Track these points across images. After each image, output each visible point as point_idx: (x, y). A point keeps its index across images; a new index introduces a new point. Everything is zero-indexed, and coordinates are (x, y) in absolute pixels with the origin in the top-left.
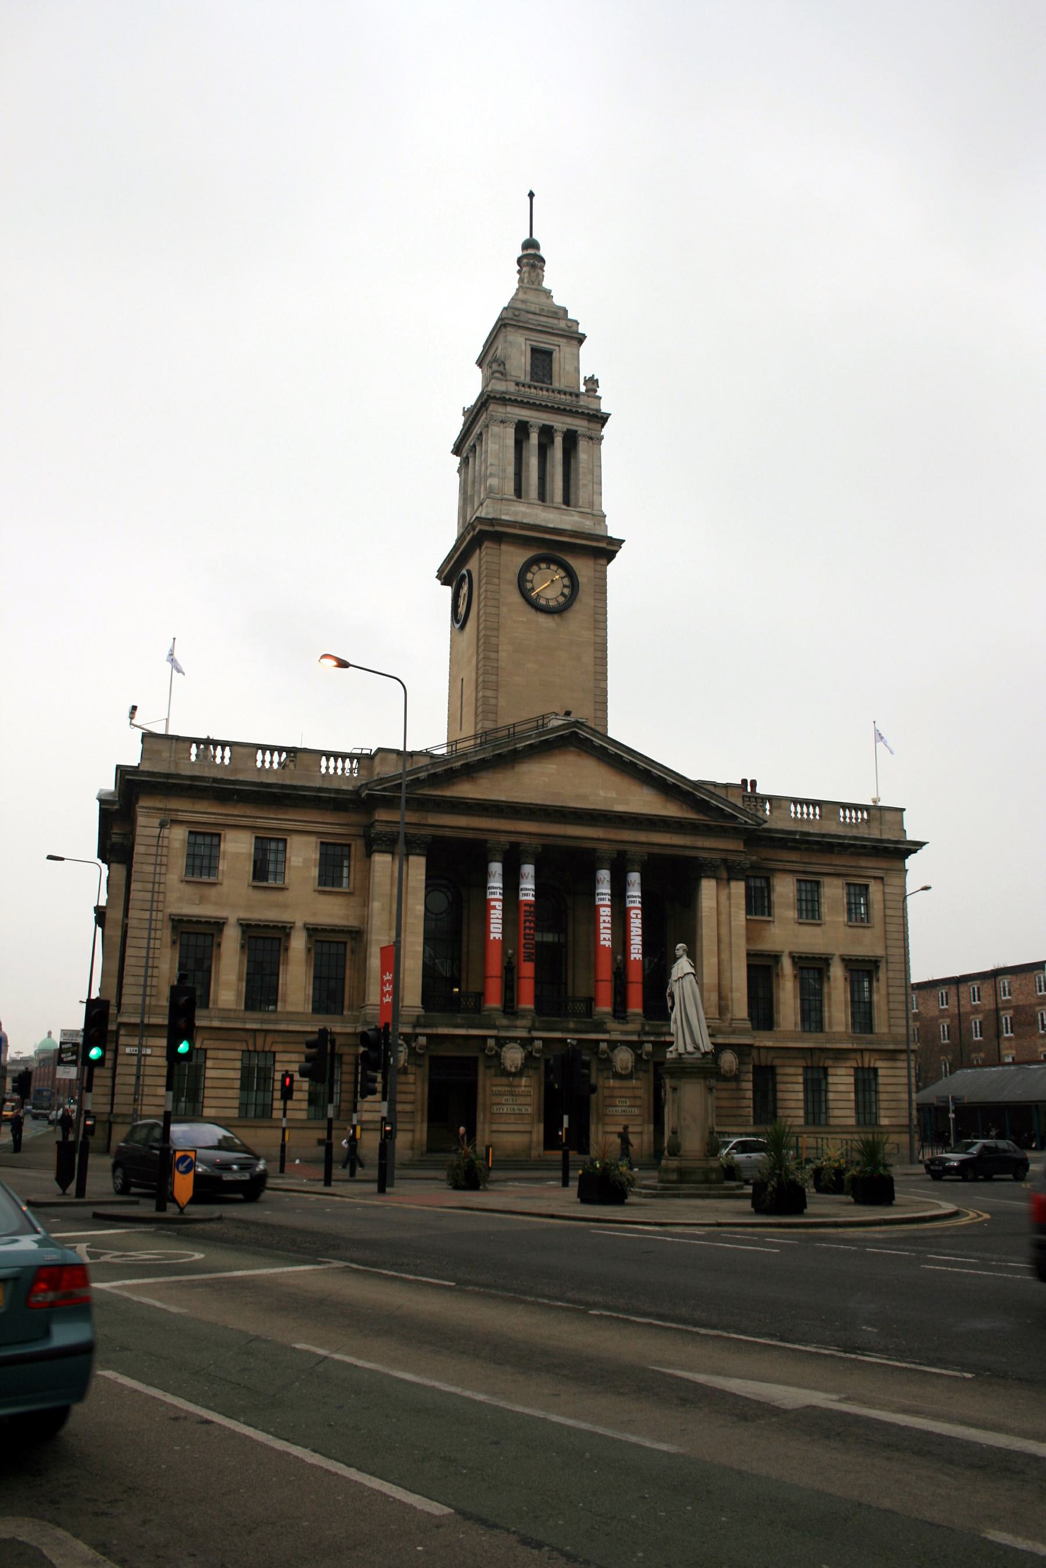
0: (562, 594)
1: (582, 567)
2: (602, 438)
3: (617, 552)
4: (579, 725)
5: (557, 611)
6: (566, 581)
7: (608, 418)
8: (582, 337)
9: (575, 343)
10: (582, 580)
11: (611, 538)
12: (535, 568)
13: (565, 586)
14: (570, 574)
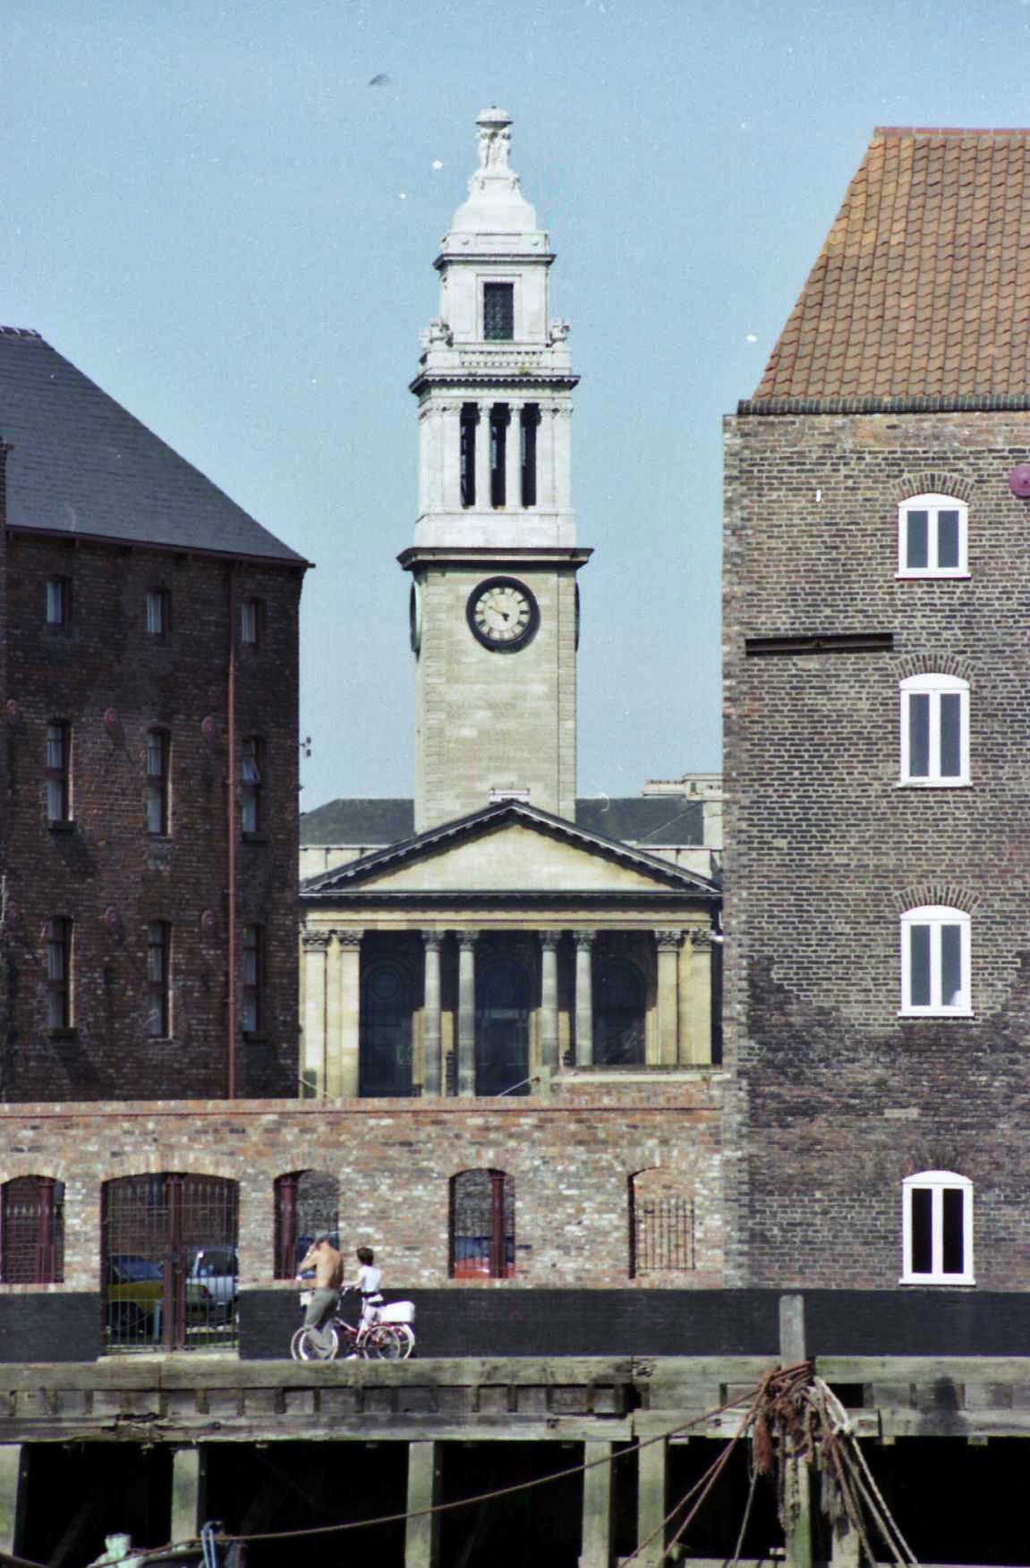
0: (519, 623)
5: (515, 645)
6: (525, 606)
10: (541, 601)
12: (485, 597)
13: (522, 612)
14: (528, 595)
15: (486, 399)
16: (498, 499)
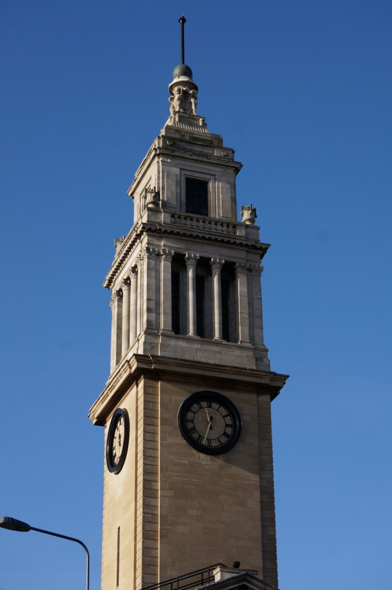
0: (225, 434)
1: (244, 402)
2: (260, 270)
3: (280, 388)
4: (250, 579)
7: (267, 249)
8: (238, 166)
9: (231, 171)
11: (275, 374)
13: (227, 426)
14: (232, 411)
15: (193, 253)
16: (203, 329)
